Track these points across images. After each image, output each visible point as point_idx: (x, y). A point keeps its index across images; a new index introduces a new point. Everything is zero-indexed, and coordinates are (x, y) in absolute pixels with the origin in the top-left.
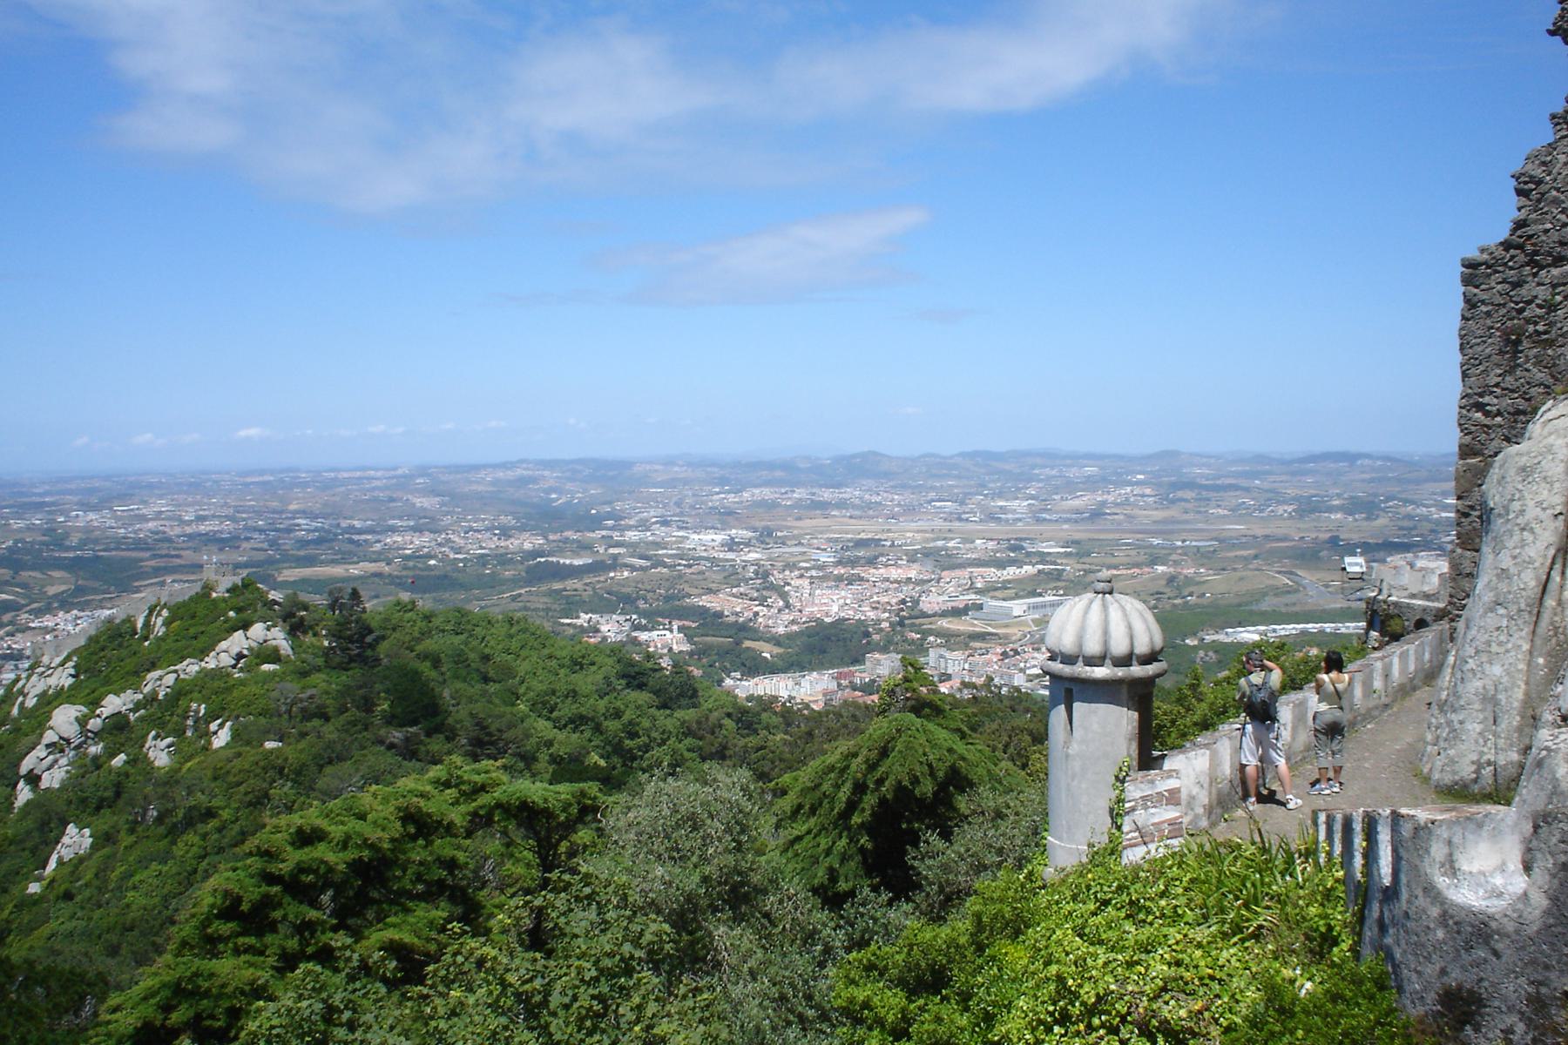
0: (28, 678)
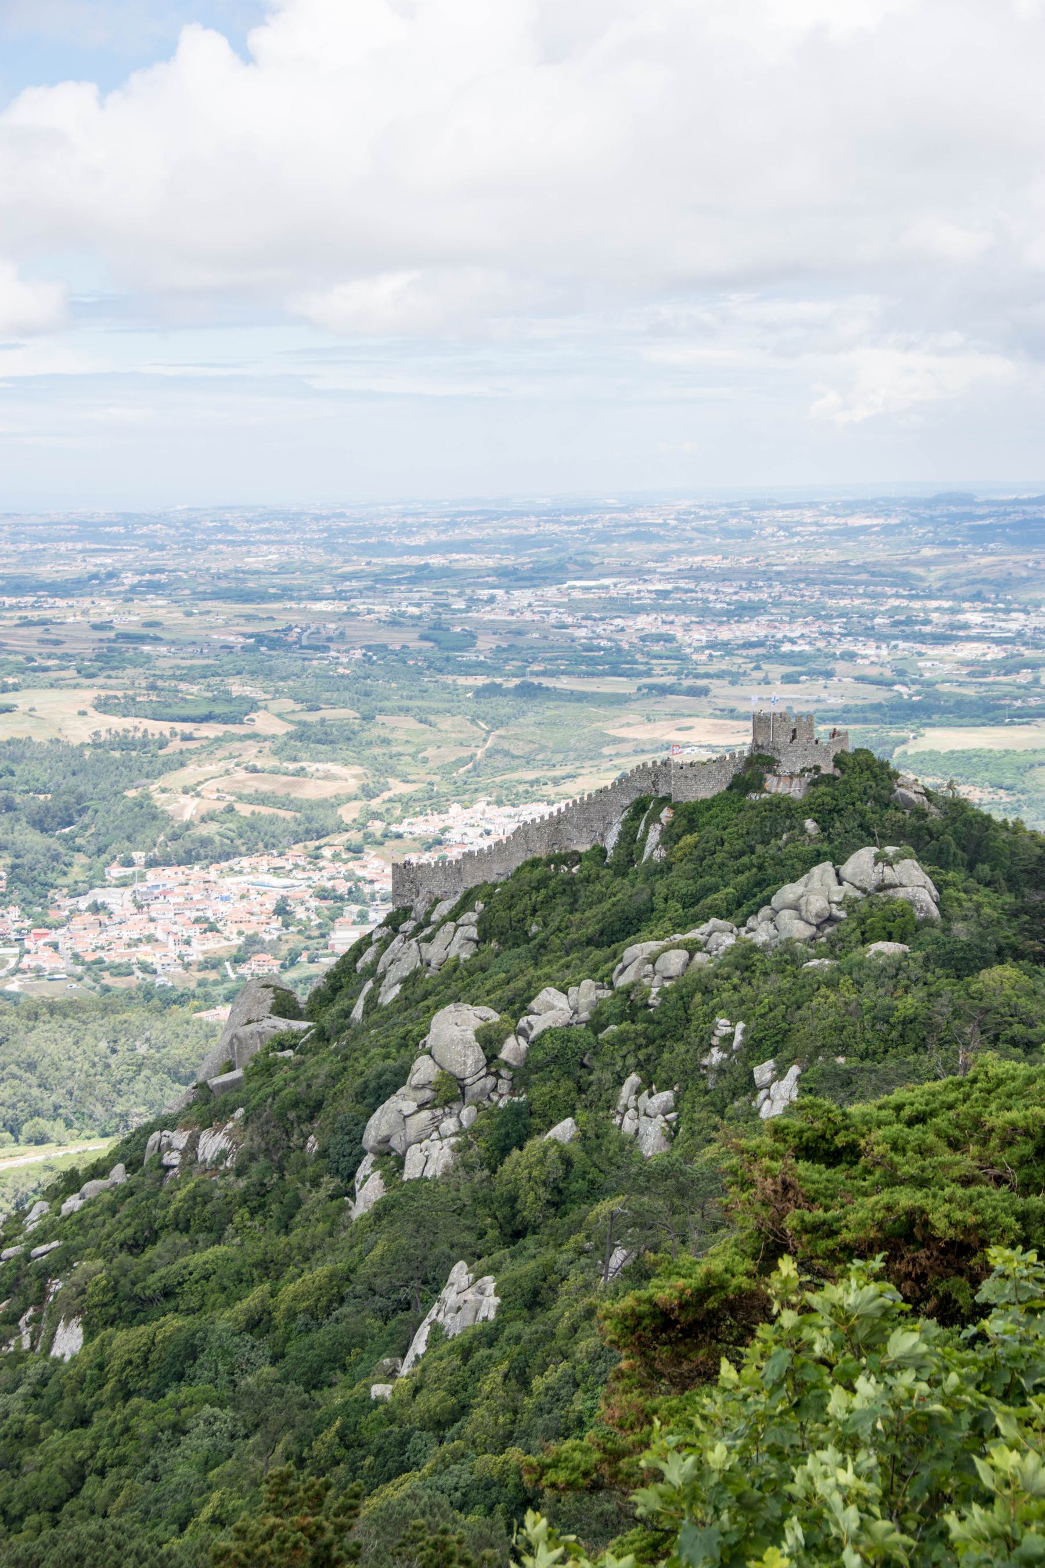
0: (385, 943)
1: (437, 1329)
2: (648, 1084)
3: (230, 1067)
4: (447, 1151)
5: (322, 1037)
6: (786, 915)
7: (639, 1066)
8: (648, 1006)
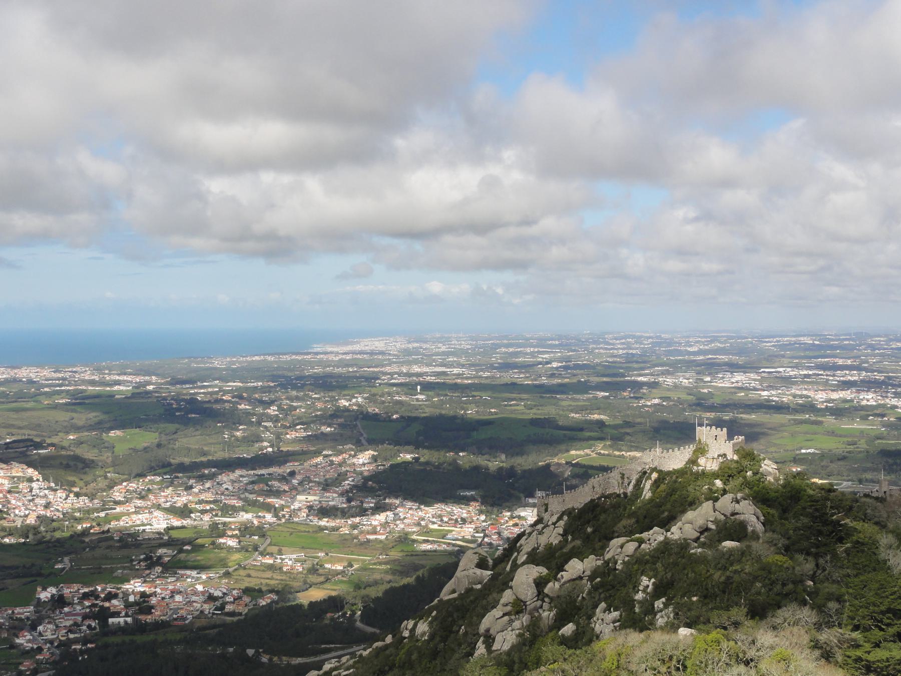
2: (608, 610)
3: (454, 591)
4: (514, 636)
5: (493, 578)
6: (688, 527)
7: (605, 600)
8: (615, 569)
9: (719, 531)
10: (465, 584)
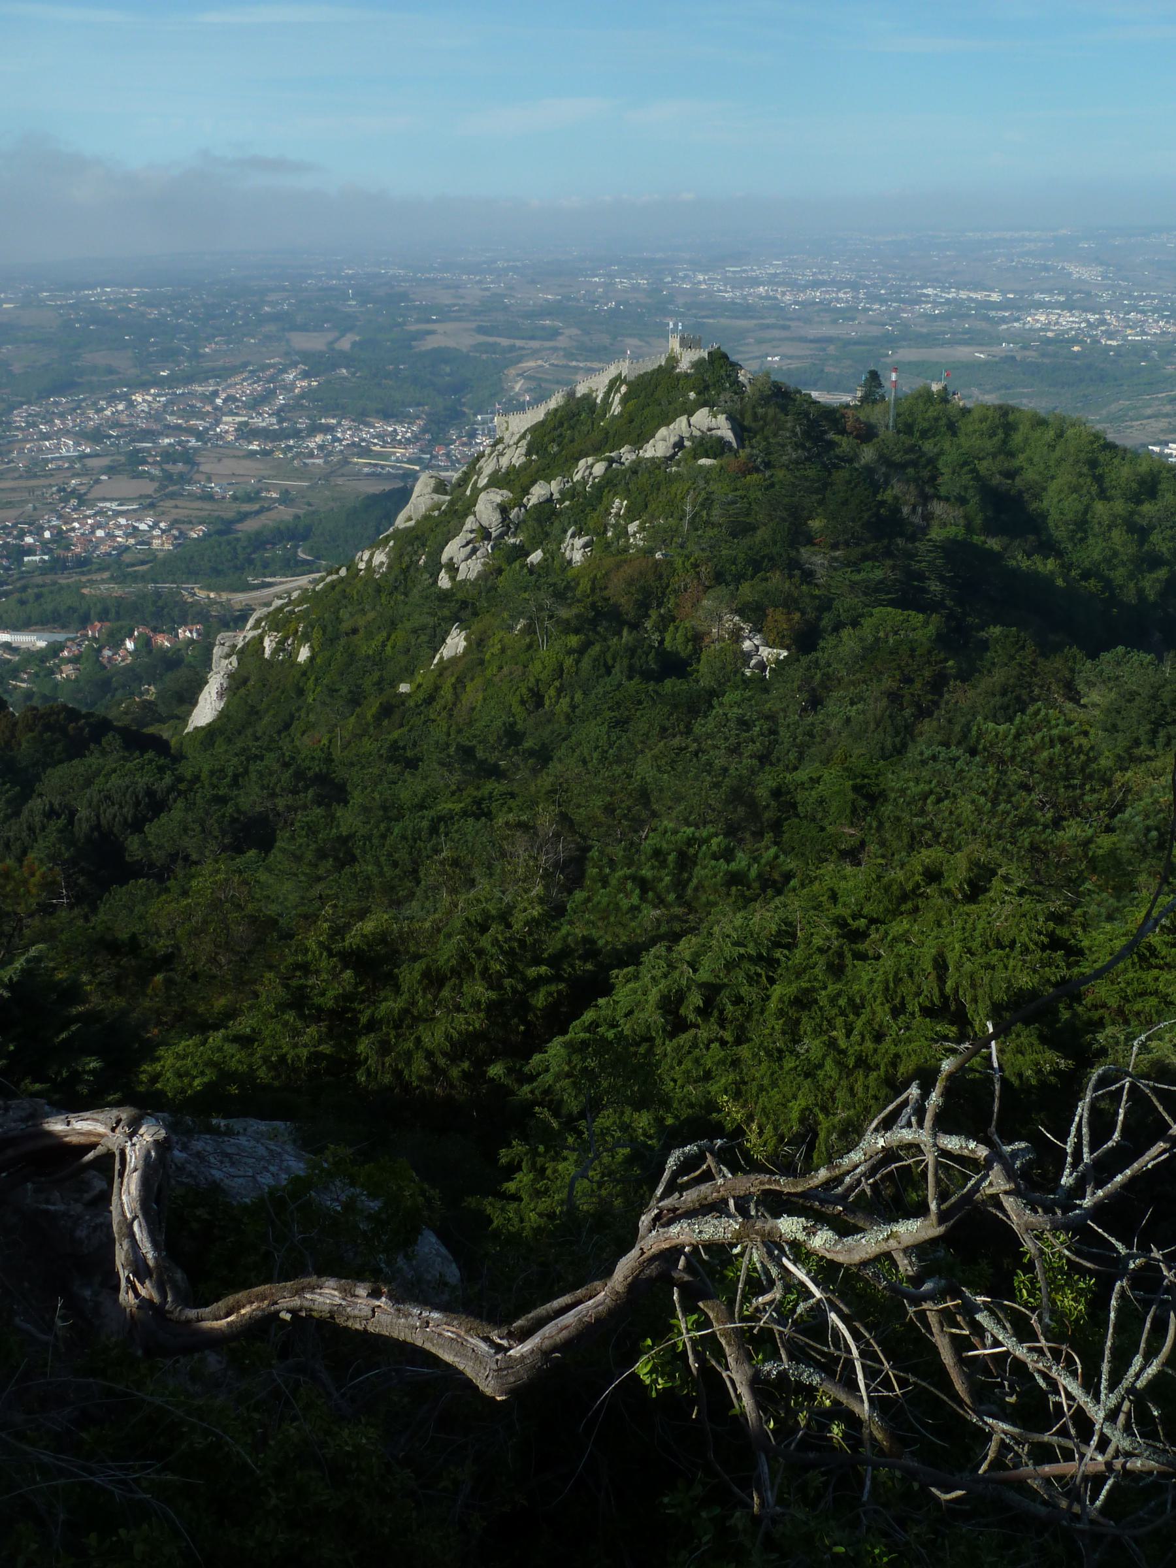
1: (441, 658)
3: (410, 519)
7: (575, 523)
9: (694, 449)
10: (422, 510)
